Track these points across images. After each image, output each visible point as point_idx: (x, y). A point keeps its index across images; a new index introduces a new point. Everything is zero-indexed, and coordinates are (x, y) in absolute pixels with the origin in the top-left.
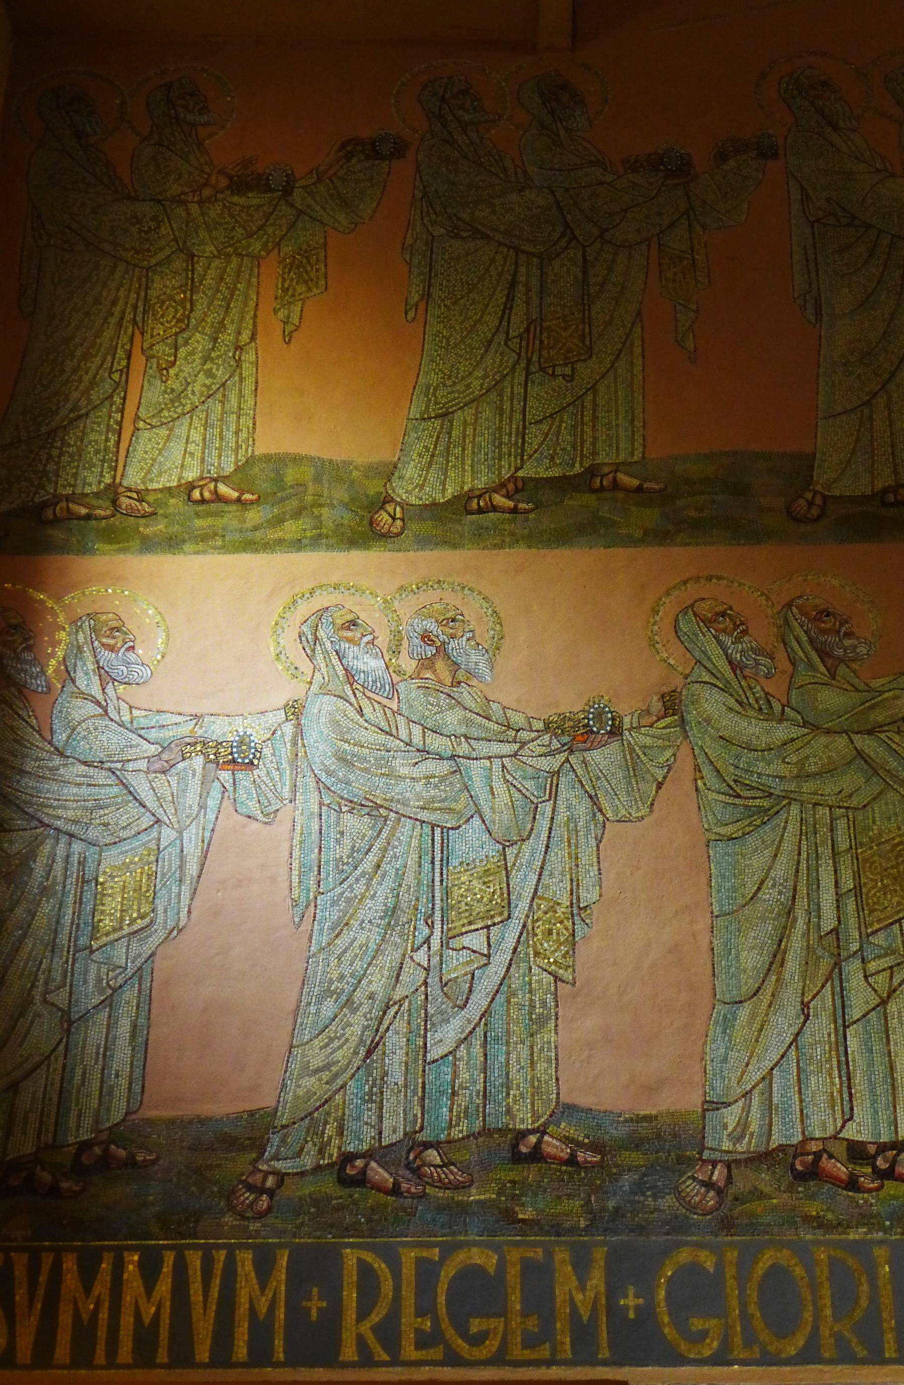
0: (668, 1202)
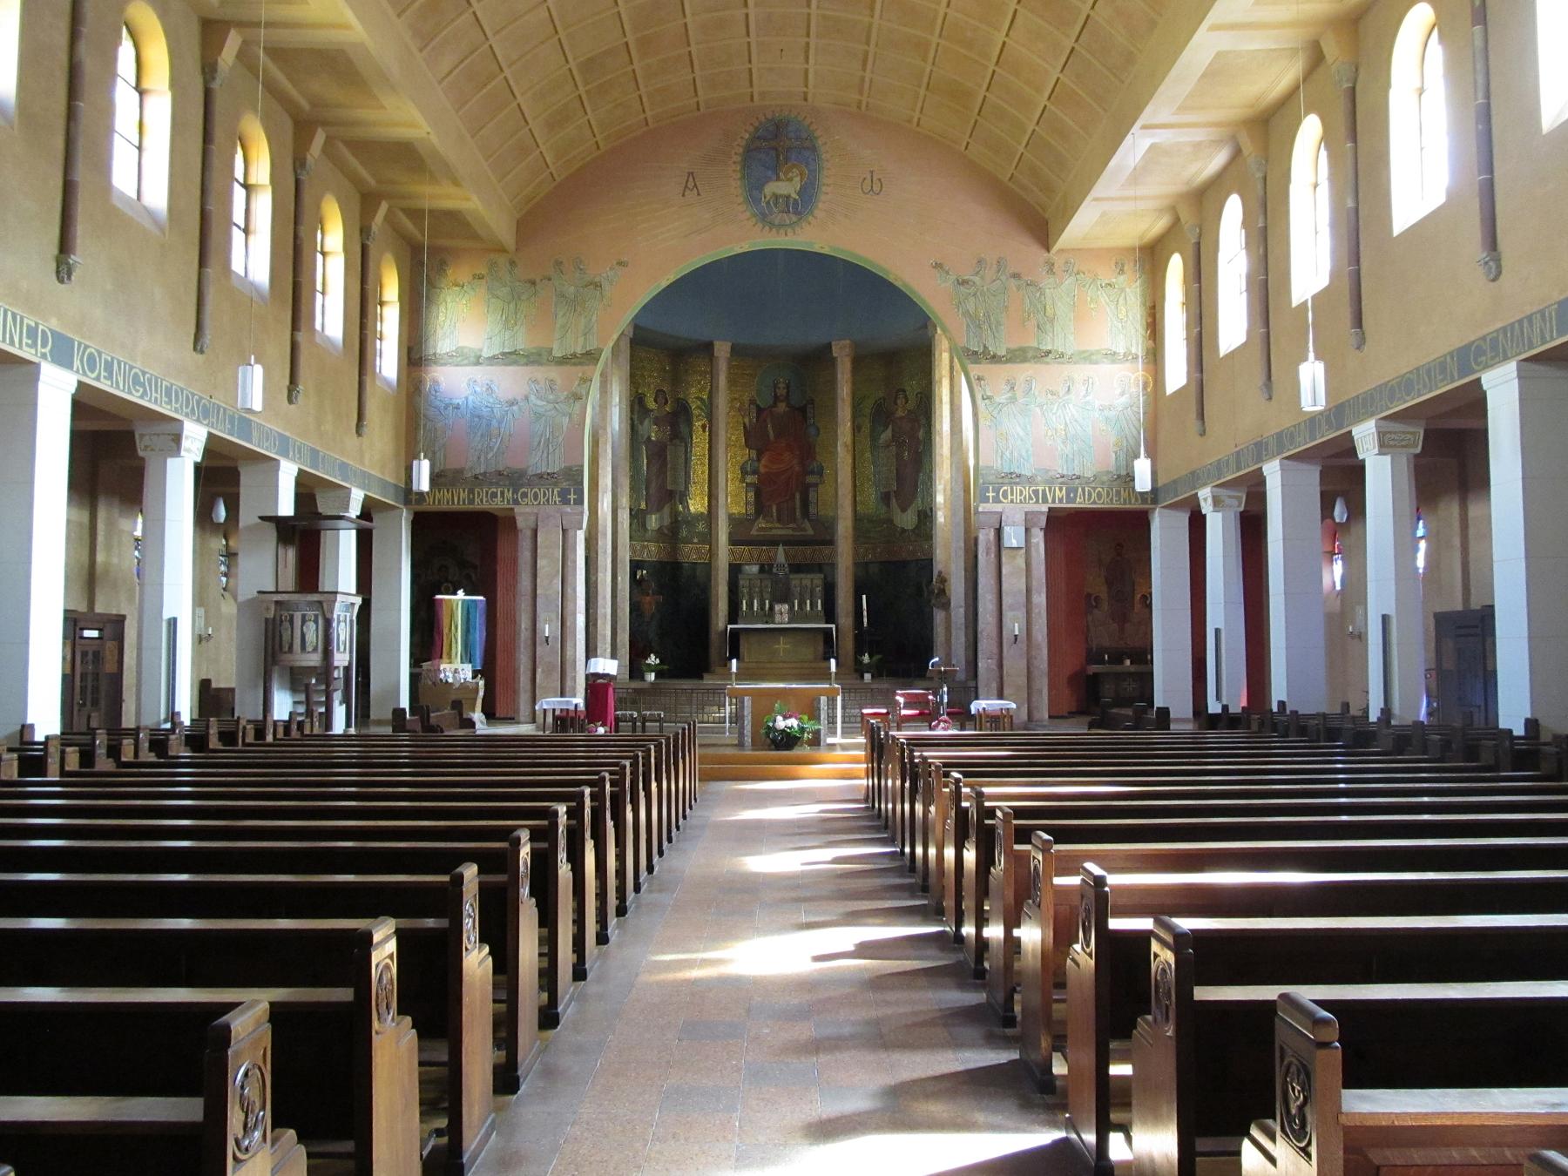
0: (521, 482)
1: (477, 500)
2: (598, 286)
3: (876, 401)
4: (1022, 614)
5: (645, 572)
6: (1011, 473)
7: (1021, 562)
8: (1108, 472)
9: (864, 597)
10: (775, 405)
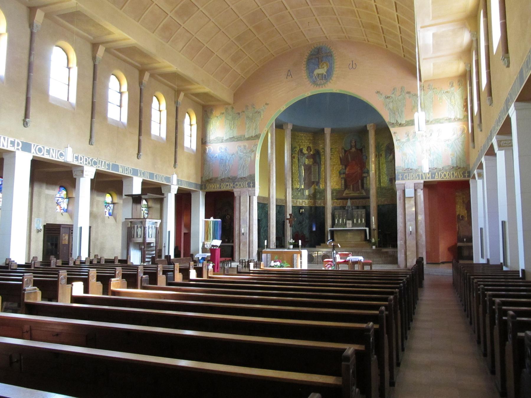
1: (222, 187)
2: (259, 112)
4: (414, 223)
5: (303, 210)
6: (408, 169)
7: (413, 202)
8: (449, 166)
10: (351, 149)
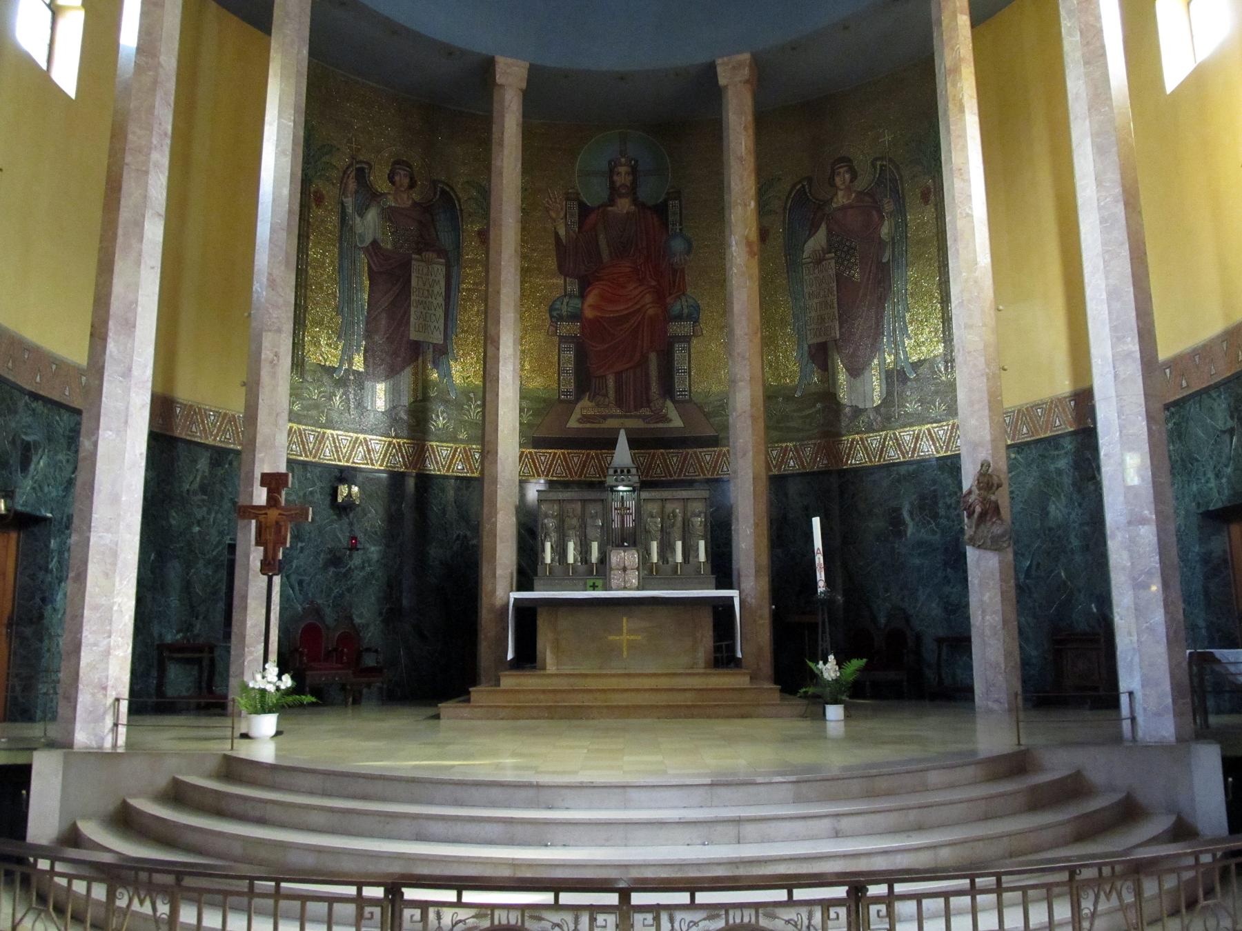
3: (794, 186)
5: (355, 489)
9: (816, 521)
10: (612, 202)
